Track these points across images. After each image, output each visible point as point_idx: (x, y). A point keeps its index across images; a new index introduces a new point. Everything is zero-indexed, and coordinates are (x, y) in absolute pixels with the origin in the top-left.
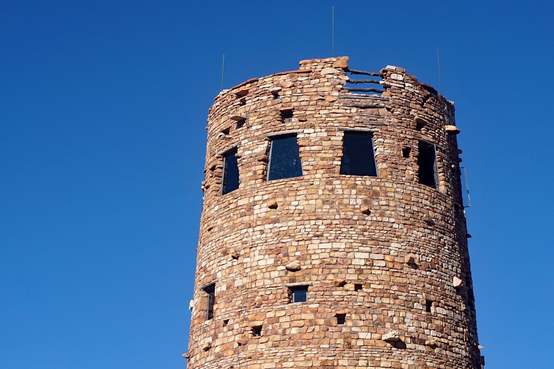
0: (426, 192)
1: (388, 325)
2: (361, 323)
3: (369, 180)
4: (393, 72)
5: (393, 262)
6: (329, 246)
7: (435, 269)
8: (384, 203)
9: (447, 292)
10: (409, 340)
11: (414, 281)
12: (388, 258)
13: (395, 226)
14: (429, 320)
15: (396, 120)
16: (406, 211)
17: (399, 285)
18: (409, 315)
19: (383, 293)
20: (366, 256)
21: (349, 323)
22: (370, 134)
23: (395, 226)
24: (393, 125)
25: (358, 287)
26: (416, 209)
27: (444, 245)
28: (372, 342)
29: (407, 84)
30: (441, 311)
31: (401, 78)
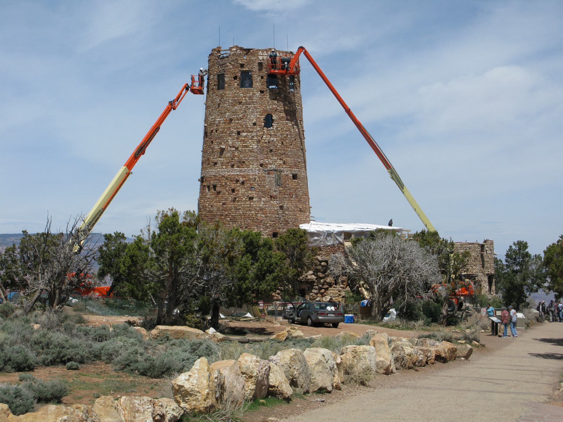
0: (242, 91)
1: (223, 143)
2: (216, 143)
3: (221, 92)
4: (232, 48)
5: (226, 120)
6: (211, 118)
7: (243, 119)
8: (225, 99)
9: (249, 126)
10: (229, 147)
11: (233, 126)
12: (225, 119)
13: (228, 107)
14: (238, 138)
15: (232, 67)
16: (232, 100)
17: (227, 128)
18: (230, 138)
19: (222, 132)
20: (219, 119)
21: (213, 144)
22: (223, 74)
23: (228, 107)
24: (230, 69)
25: (216, 131)
26: (236, 98)
27: (250, 108)
28: (218, 150)
29: (238, 51)
30: (244, 134)
31: (235, 49)
